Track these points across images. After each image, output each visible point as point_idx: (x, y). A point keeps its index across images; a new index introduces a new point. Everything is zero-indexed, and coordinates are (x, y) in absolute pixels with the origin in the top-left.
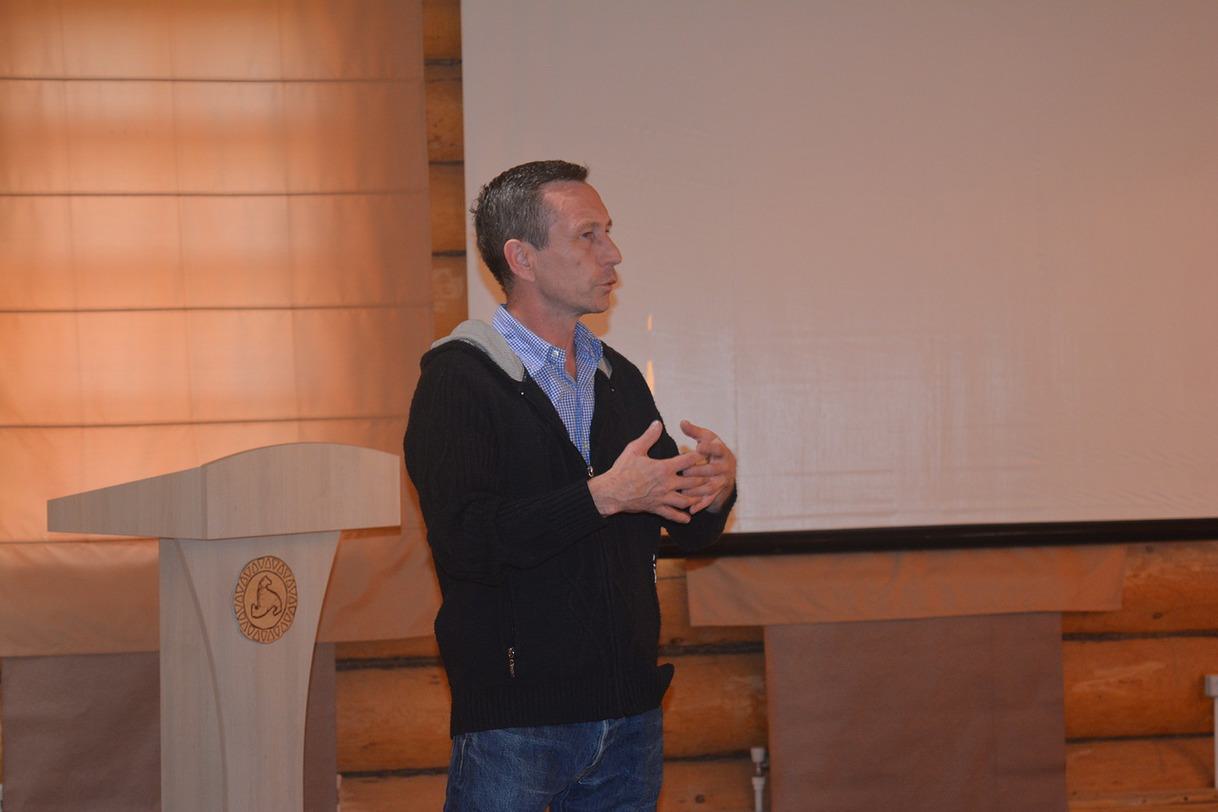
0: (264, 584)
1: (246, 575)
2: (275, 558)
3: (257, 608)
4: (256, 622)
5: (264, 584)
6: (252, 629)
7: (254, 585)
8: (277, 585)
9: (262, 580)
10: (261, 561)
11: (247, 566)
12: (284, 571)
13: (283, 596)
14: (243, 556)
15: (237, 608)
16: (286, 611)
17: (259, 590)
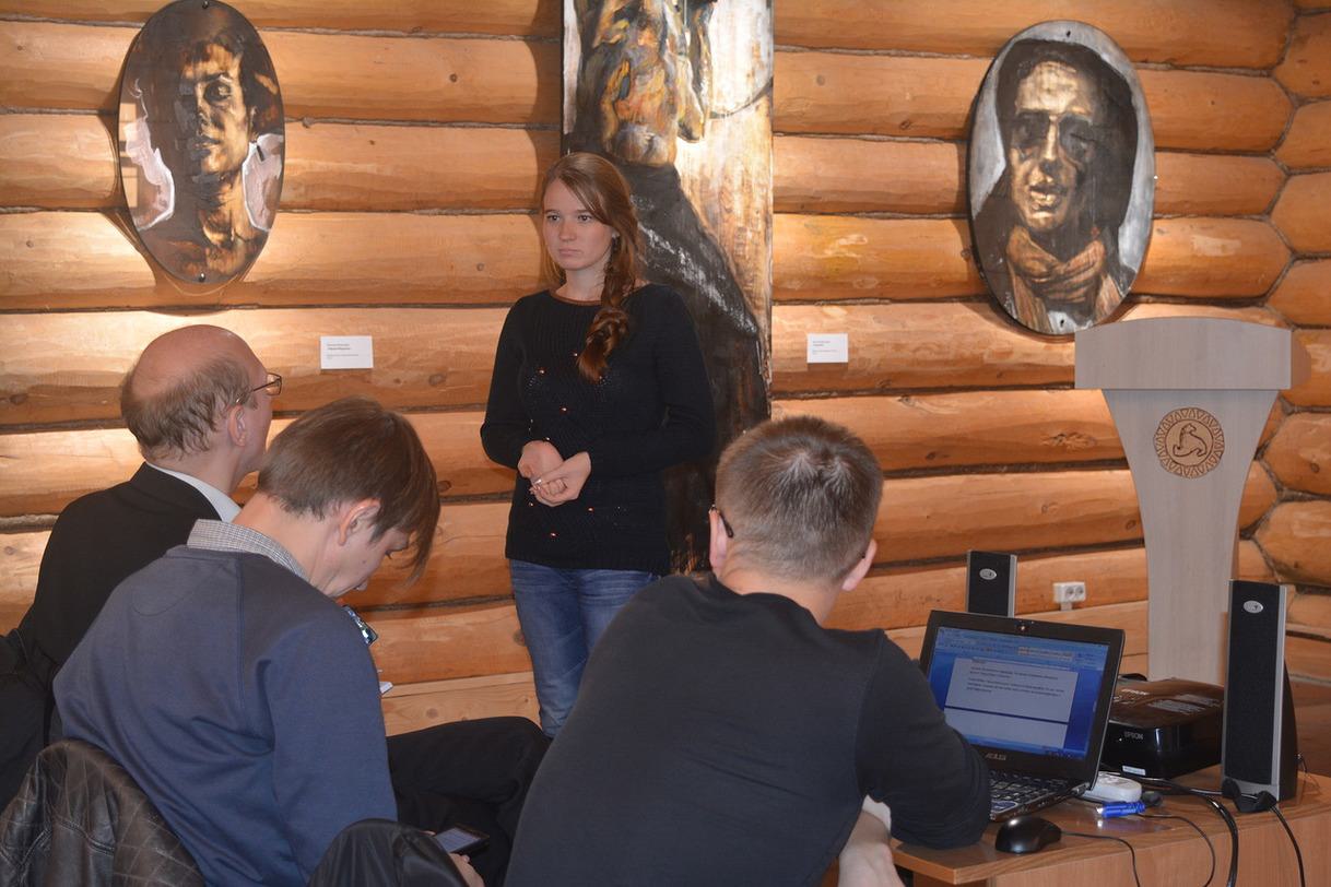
0: (1188, 430)
1: (1169, 422)
2: (1199, 410)
3: (1179, 448)
4: (1177, 459)
5: (1188, 430)
6: (1174, 465)
7: (1176, 430)
8: (1202, 431)
9: (1186, 426)
10: (1184, 412)
11: (1170, 414)
12: (1211, 423)
13: (1209, 441)
14: (1165, 407)
15: (1159, 447)
16: (1212, 453)
17: (1182, 434)
